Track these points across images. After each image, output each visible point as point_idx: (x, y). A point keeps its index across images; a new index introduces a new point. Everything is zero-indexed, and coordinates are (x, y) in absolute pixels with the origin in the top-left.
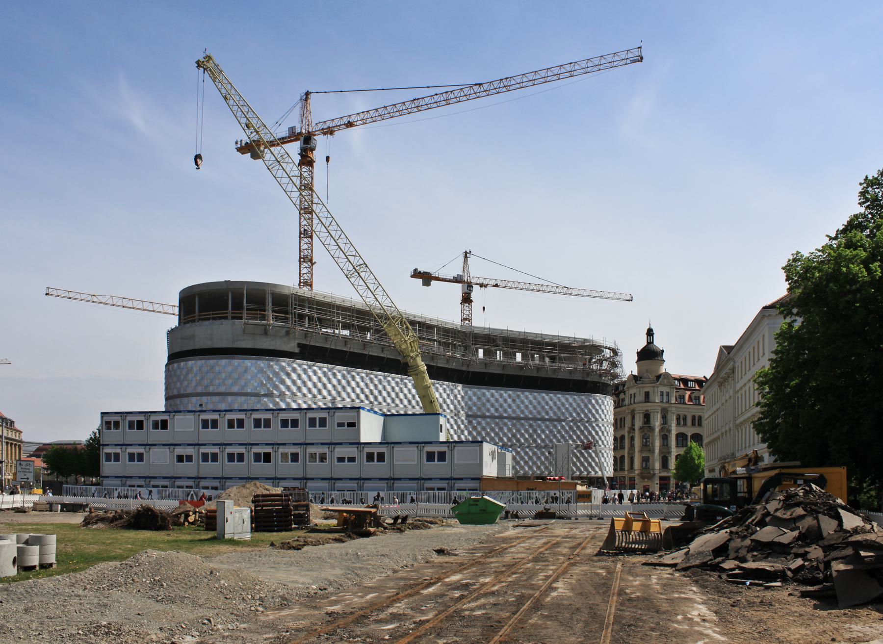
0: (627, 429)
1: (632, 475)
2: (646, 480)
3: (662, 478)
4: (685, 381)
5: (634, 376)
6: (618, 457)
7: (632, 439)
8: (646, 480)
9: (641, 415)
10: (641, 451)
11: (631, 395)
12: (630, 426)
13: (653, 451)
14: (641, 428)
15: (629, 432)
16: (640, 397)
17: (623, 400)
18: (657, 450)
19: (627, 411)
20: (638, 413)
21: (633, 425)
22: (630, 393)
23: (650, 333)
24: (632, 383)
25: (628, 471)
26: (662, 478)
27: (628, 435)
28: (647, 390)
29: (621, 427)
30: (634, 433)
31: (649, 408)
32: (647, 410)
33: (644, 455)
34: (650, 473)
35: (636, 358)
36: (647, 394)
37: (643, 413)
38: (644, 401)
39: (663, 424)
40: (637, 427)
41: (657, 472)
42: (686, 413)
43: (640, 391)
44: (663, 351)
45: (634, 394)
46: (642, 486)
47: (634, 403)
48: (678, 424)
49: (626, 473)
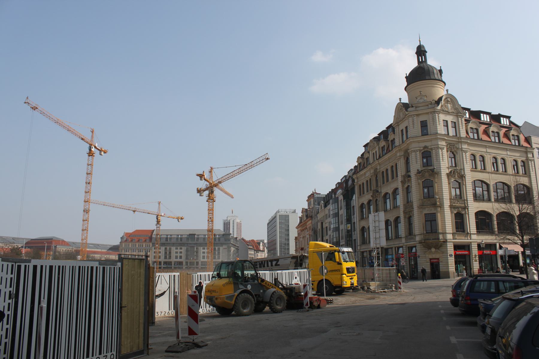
0: (400, 178)
1: (411, 243)
2: (433, 250)
3: (457, 247)
4: (476, 114)
5: (404, 104)
6: (392, 219)
7: (408, 190)
8: (433, 250)
9: (418, 153)
10: (422, 206)
11: (402, 131)
12: (404, 173)
13: (441, 206)
14: (419, 172)
15: (403, 182)
16: (415, 130)
17: (393, 141)
18: (447, 203)
19: (398, 154)
20: (414, 151)
21: (408, 170)
22: (401, 129)
23: (421, 52)
24: (401, 114)
25: (406, 237)
26: (457, 247)
27: (403, 186)
28: (423, 118)
29: (393, 178)
30: (409, 181)
31: (428, 144)
32: (425, 147)
33: (426, 211)
34: (438, 239)
35: (406, 84)
36: (424, 125)
37: (420, 150)
38: (421, 135)
39: (452, 166)
40: (413, 173)
41: (449, 237)
42: (483, 154)
43: (413, 121)
44: (441, 71)
45: (406, 128)
46: (428, 260)
47: (407, 138)
48: (475, 169)
49: (403, 240)
